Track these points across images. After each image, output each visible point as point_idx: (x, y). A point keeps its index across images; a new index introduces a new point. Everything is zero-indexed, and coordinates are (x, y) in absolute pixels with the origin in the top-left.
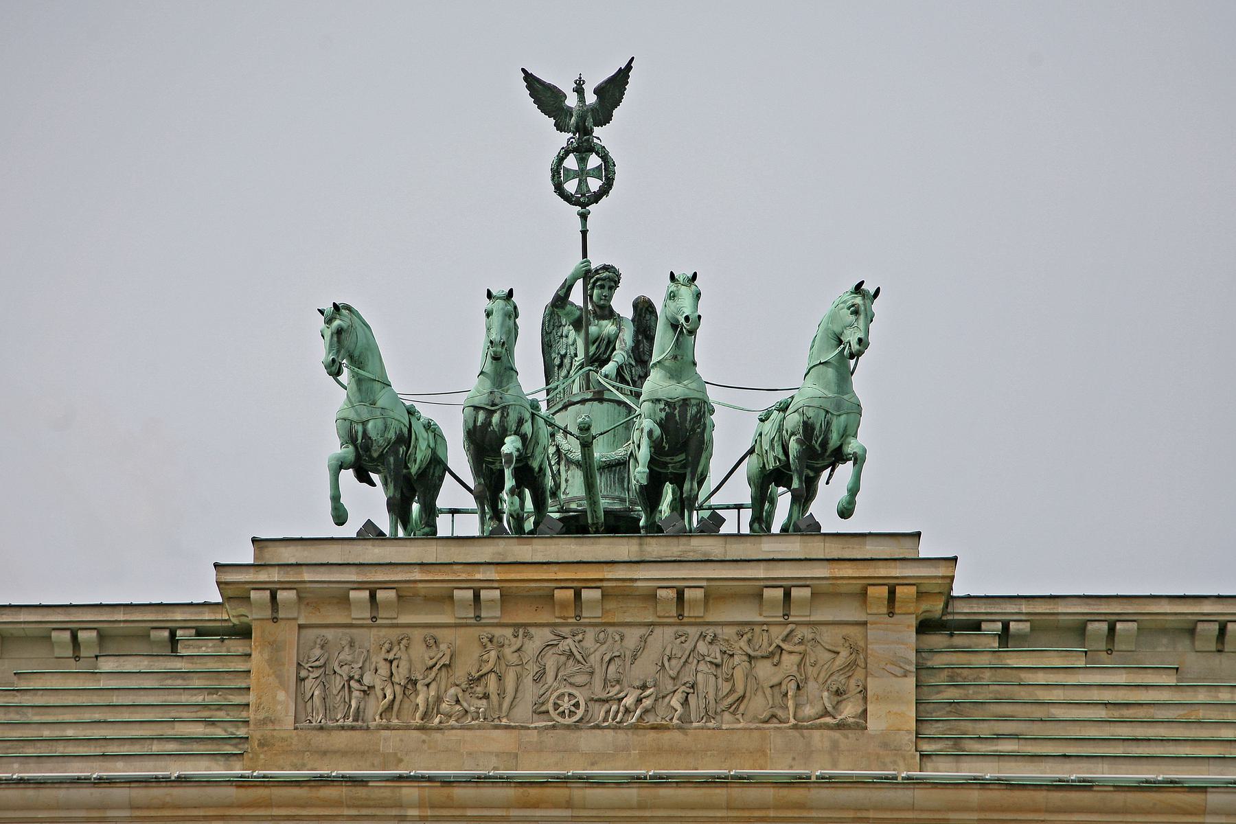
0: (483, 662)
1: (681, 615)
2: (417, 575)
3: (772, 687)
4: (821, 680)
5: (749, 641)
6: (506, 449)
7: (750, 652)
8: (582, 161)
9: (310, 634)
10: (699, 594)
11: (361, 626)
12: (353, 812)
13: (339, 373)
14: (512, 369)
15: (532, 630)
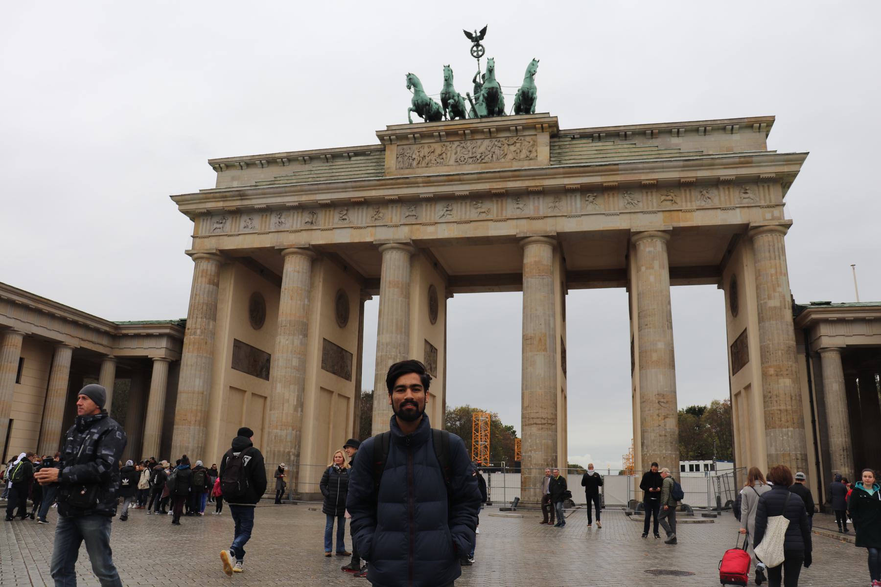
0: (442, 150)
1: (491, 136)
2: (424, 129)
3: (514, 151)
4: (526, 148)
5: (508, 141)
6: (449, 101)
7: (507, 143)
8: (477, 48)
9: (400, 147)
10: (494, 129)
11: (413, 144)
12: (406, 186)
13: (410, 88)
14: (453, 85)
15: (454, 142)
